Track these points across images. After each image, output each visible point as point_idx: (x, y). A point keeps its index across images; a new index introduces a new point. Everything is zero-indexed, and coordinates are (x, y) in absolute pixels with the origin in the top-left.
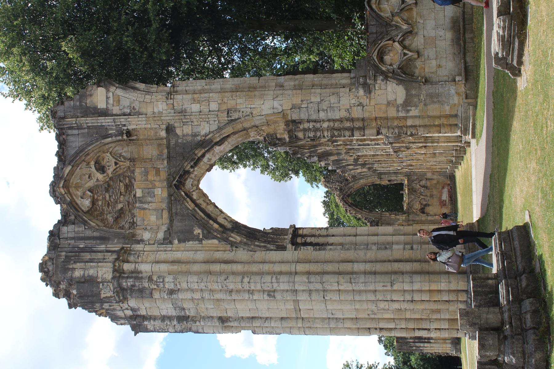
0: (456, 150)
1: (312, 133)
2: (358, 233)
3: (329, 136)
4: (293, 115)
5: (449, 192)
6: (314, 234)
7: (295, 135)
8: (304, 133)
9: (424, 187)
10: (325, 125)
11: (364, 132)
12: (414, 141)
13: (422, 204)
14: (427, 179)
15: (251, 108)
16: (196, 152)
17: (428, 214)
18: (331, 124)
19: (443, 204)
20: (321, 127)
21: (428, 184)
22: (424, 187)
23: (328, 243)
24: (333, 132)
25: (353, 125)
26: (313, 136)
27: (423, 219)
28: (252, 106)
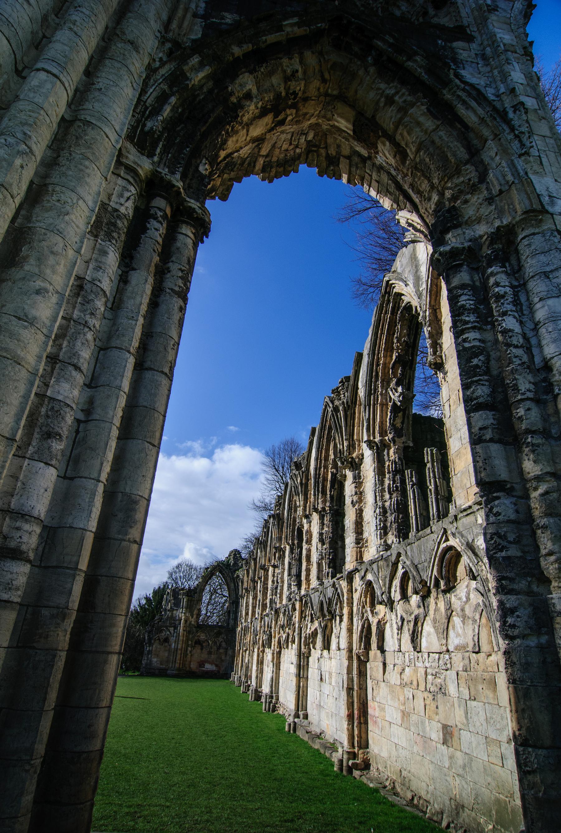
0: (271, 697)
1: (471, 302)
2: (148, 375)
3: (467, 345)
4: (538, 238)
5: (212, 671)
6: (174, 259)
7: (461, 265)
8: (468, 285)
9: (220, 645)
10: (510, 323)
11: (491, 440)
12: (303, 635)
13: (204, 642)
14: (227, 649)
15: (539, 156)
16: (418, 58)
17: (193, 647)
18: (518, 340)
19: (201, 664)
20: (505, 314)
21: (221, 651)
22: (220, 645)
23: (134, 269)
24: (481, 354)
25: (522, 400)
26: (463, 306)
27: (190, 642)
28: (544, 160)
